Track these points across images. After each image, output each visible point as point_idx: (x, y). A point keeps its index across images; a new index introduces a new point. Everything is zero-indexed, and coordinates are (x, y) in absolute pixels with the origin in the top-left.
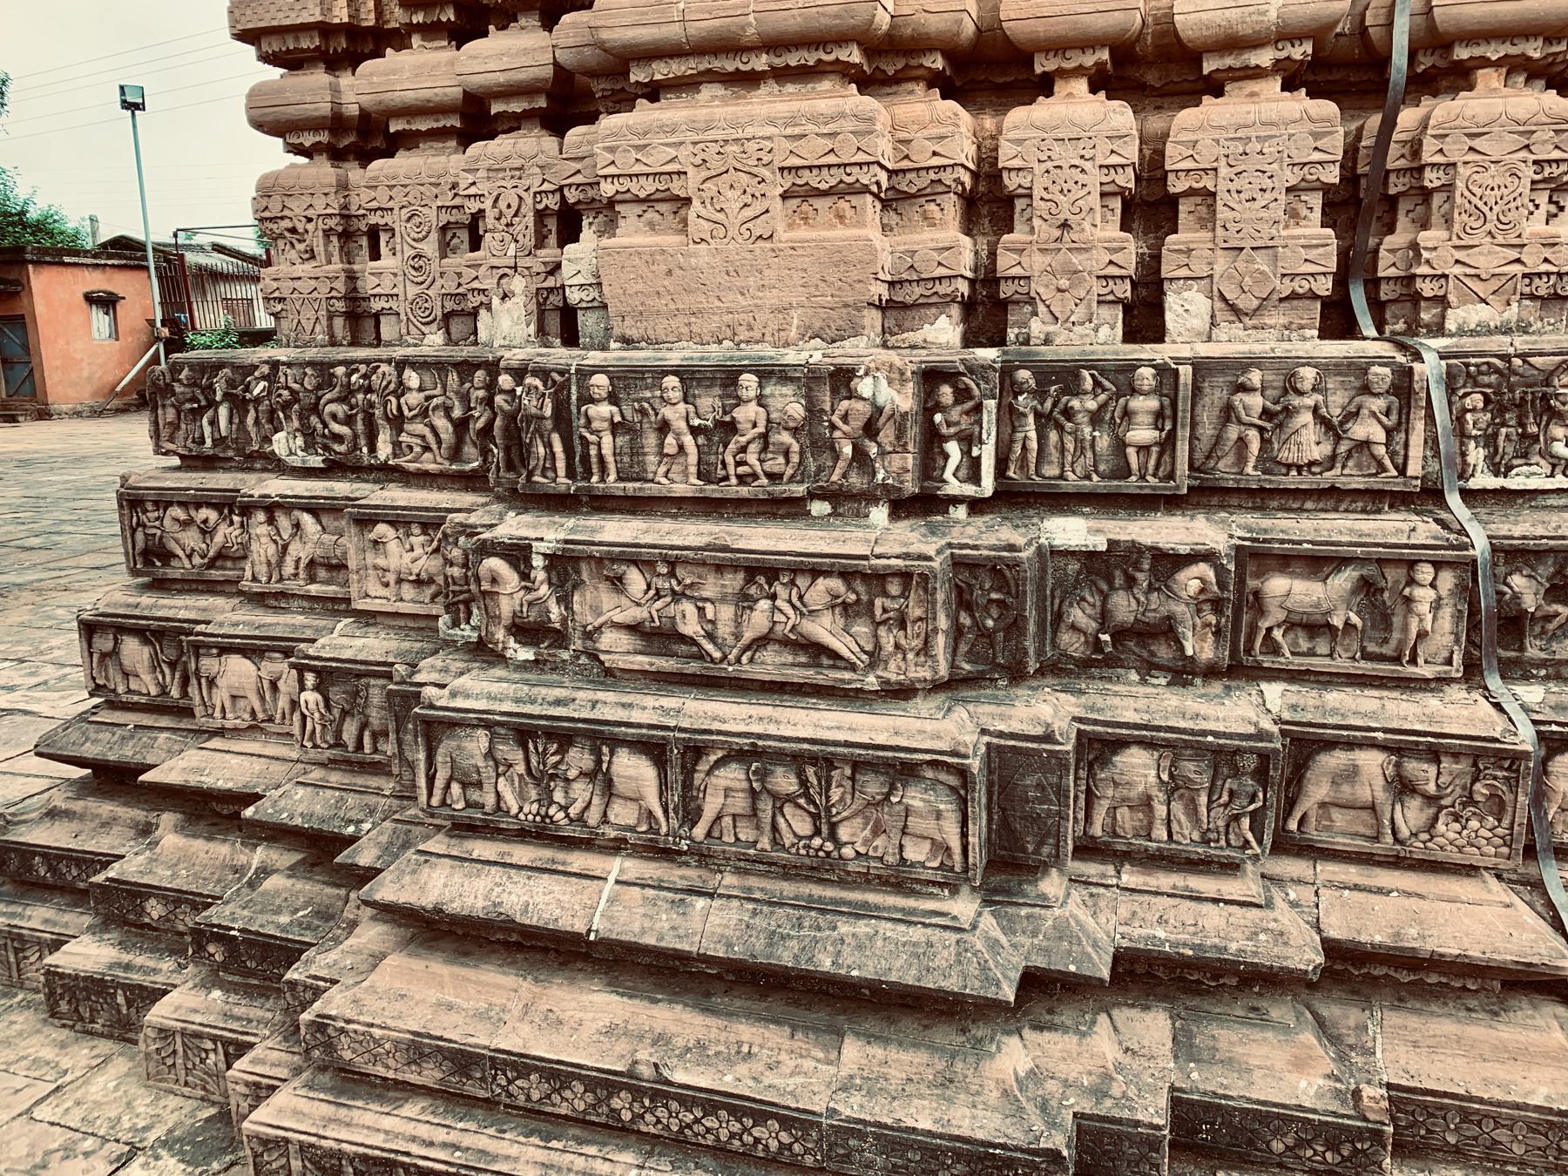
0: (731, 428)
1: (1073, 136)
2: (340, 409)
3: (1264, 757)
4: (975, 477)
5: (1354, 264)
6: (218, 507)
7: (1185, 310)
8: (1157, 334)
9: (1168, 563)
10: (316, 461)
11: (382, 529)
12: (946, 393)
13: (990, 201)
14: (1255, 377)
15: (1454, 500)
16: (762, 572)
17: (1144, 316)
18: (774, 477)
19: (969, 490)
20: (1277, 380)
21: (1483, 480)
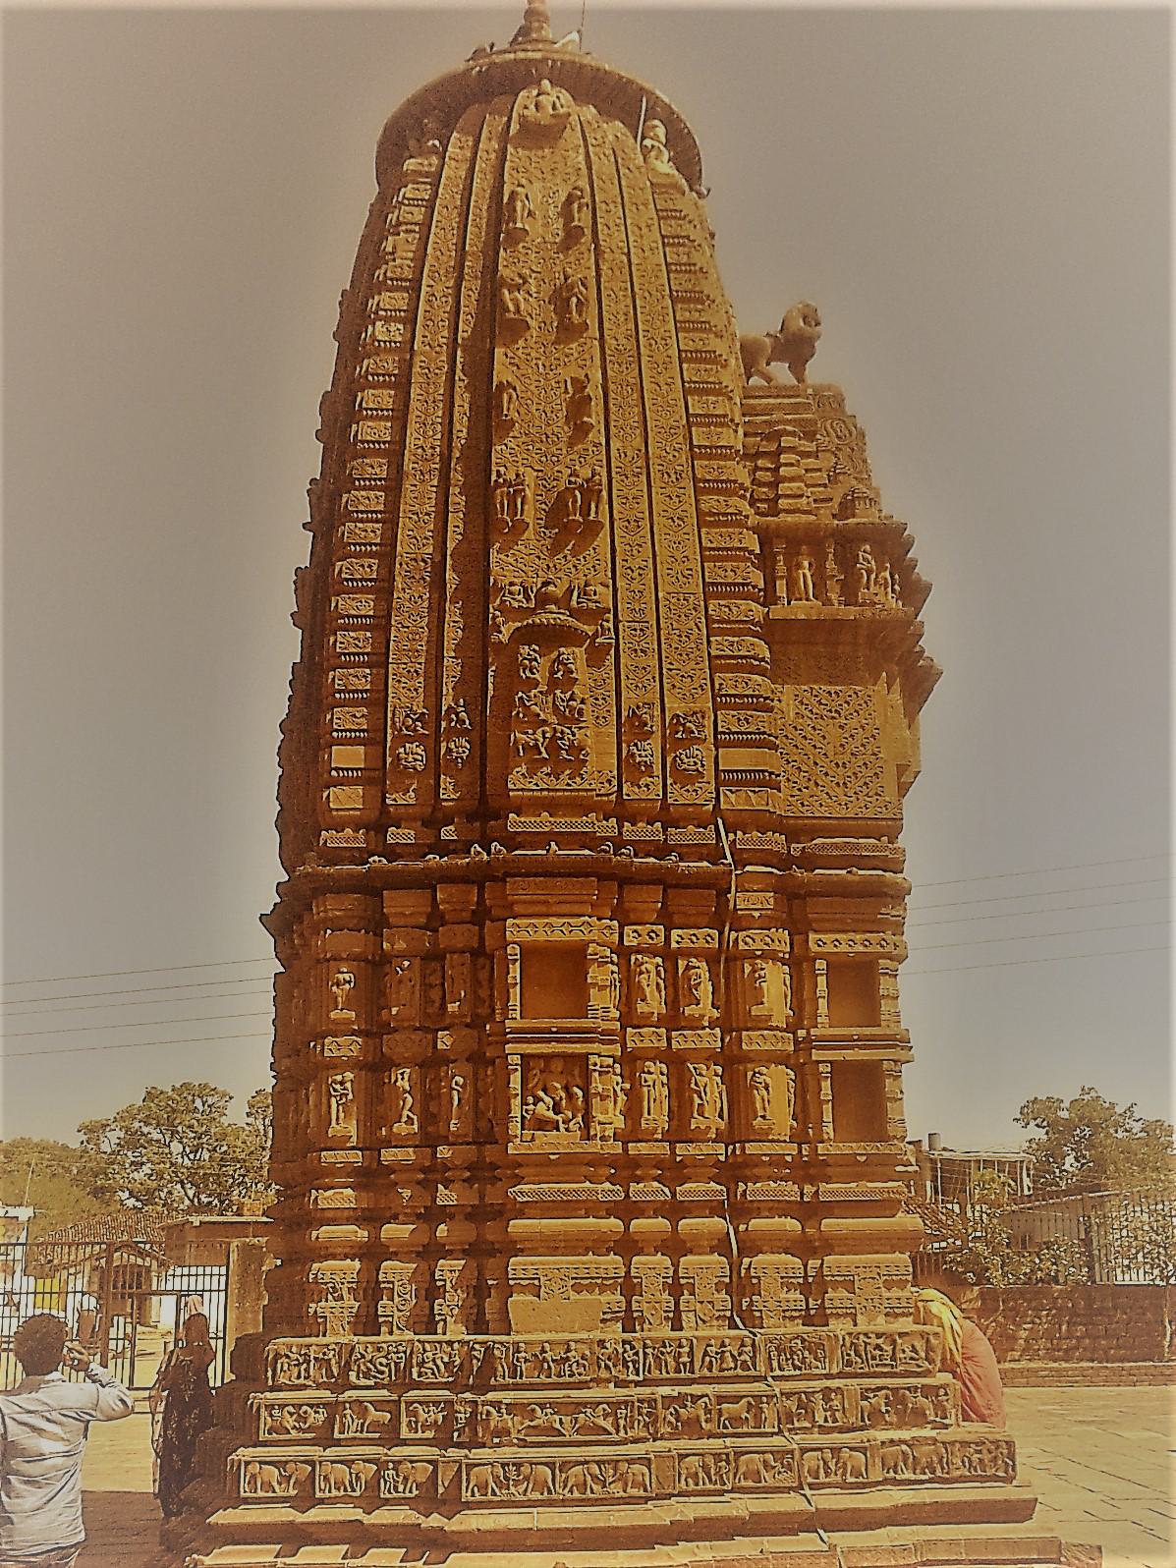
0: (568, 1359)
1: (652, 1266)
2: (384, 1361)
3: (727, 1455)
4: (638, 1374)
5: (736, 1307)
6: (311, 1406)
7: (687, 1319)
8: (681, 1329)
9: (695, 1398)
10: (371, 1383)
11: (415, 1405)
12: (628, 1347)
13: (629, 1287)
14: (713, 1342)
15: (769, 1379)
16: (581, 1405)
17: (677, 1326)
18: (580, 1375)
19: (636, 1378)
20: (719, 1343)
21: (778, 1373)
